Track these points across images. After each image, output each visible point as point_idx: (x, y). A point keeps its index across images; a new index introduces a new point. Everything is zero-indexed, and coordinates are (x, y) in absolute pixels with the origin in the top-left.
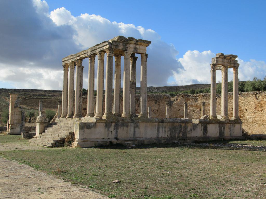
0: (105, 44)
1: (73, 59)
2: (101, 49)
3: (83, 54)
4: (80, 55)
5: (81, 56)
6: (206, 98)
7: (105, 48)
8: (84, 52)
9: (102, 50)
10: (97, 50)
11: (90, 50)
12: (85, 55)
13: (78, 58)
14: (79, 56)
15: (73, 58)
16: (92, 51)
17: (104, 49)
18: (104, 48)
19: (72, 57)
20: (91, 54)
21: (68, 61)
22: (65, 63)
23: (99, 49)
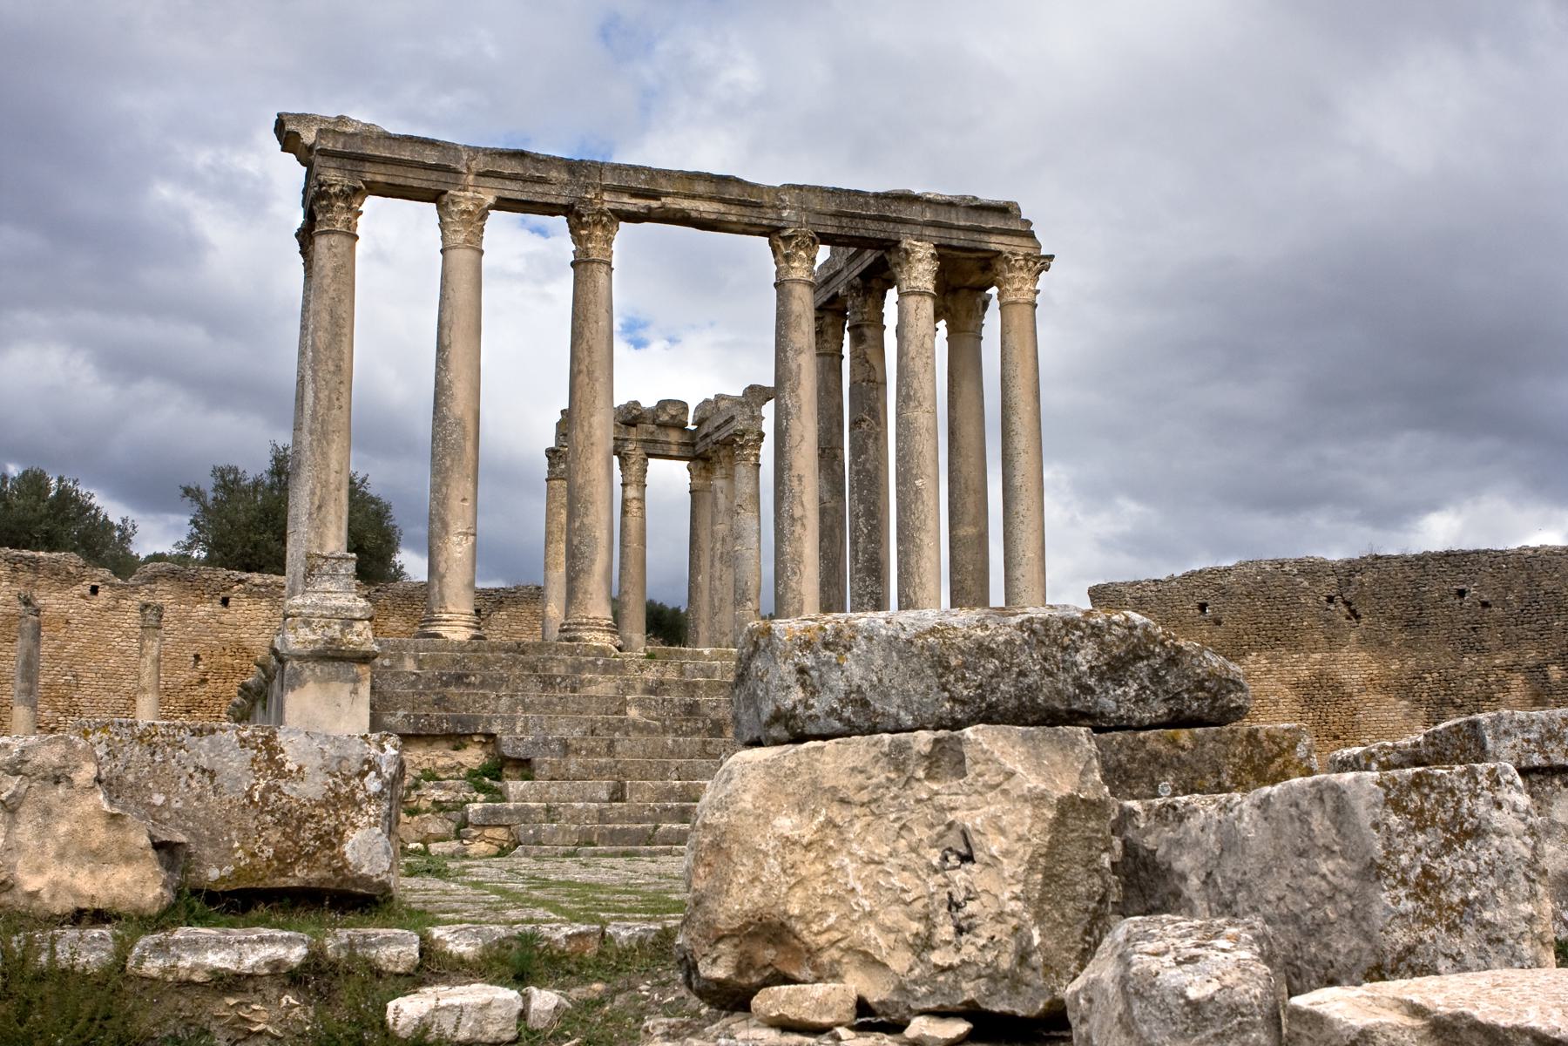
0: (992, 222)
1: (538, 188)
2: (958, 239)
3: (711, 199)
4: (667, 194)
5: (668, 201)
6: (29, 577)
7: (995, 243)
8: (734, 192)
9: (961, 243)
10: (917, 230)
11: (816, 203)
12: (747, 211)
13: (626, 199)
14: (655, 196)
15: (541, 181)
16: (837, 215)
17: (993, 247)
18: (985, 238)
19: (510, 167)
20: (830, 231)
21: (434, 176)
22: (368, 177)
23: (928, 231)
